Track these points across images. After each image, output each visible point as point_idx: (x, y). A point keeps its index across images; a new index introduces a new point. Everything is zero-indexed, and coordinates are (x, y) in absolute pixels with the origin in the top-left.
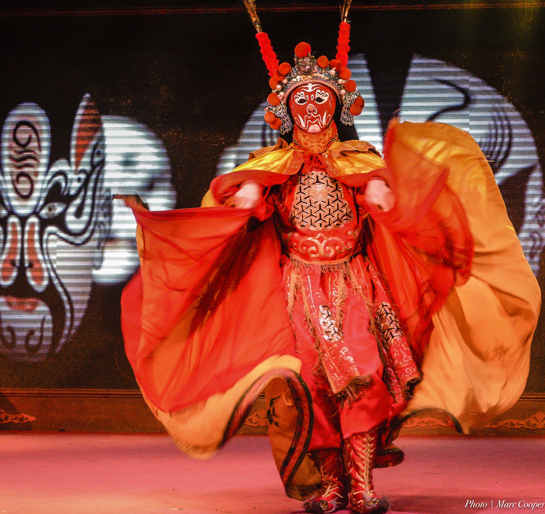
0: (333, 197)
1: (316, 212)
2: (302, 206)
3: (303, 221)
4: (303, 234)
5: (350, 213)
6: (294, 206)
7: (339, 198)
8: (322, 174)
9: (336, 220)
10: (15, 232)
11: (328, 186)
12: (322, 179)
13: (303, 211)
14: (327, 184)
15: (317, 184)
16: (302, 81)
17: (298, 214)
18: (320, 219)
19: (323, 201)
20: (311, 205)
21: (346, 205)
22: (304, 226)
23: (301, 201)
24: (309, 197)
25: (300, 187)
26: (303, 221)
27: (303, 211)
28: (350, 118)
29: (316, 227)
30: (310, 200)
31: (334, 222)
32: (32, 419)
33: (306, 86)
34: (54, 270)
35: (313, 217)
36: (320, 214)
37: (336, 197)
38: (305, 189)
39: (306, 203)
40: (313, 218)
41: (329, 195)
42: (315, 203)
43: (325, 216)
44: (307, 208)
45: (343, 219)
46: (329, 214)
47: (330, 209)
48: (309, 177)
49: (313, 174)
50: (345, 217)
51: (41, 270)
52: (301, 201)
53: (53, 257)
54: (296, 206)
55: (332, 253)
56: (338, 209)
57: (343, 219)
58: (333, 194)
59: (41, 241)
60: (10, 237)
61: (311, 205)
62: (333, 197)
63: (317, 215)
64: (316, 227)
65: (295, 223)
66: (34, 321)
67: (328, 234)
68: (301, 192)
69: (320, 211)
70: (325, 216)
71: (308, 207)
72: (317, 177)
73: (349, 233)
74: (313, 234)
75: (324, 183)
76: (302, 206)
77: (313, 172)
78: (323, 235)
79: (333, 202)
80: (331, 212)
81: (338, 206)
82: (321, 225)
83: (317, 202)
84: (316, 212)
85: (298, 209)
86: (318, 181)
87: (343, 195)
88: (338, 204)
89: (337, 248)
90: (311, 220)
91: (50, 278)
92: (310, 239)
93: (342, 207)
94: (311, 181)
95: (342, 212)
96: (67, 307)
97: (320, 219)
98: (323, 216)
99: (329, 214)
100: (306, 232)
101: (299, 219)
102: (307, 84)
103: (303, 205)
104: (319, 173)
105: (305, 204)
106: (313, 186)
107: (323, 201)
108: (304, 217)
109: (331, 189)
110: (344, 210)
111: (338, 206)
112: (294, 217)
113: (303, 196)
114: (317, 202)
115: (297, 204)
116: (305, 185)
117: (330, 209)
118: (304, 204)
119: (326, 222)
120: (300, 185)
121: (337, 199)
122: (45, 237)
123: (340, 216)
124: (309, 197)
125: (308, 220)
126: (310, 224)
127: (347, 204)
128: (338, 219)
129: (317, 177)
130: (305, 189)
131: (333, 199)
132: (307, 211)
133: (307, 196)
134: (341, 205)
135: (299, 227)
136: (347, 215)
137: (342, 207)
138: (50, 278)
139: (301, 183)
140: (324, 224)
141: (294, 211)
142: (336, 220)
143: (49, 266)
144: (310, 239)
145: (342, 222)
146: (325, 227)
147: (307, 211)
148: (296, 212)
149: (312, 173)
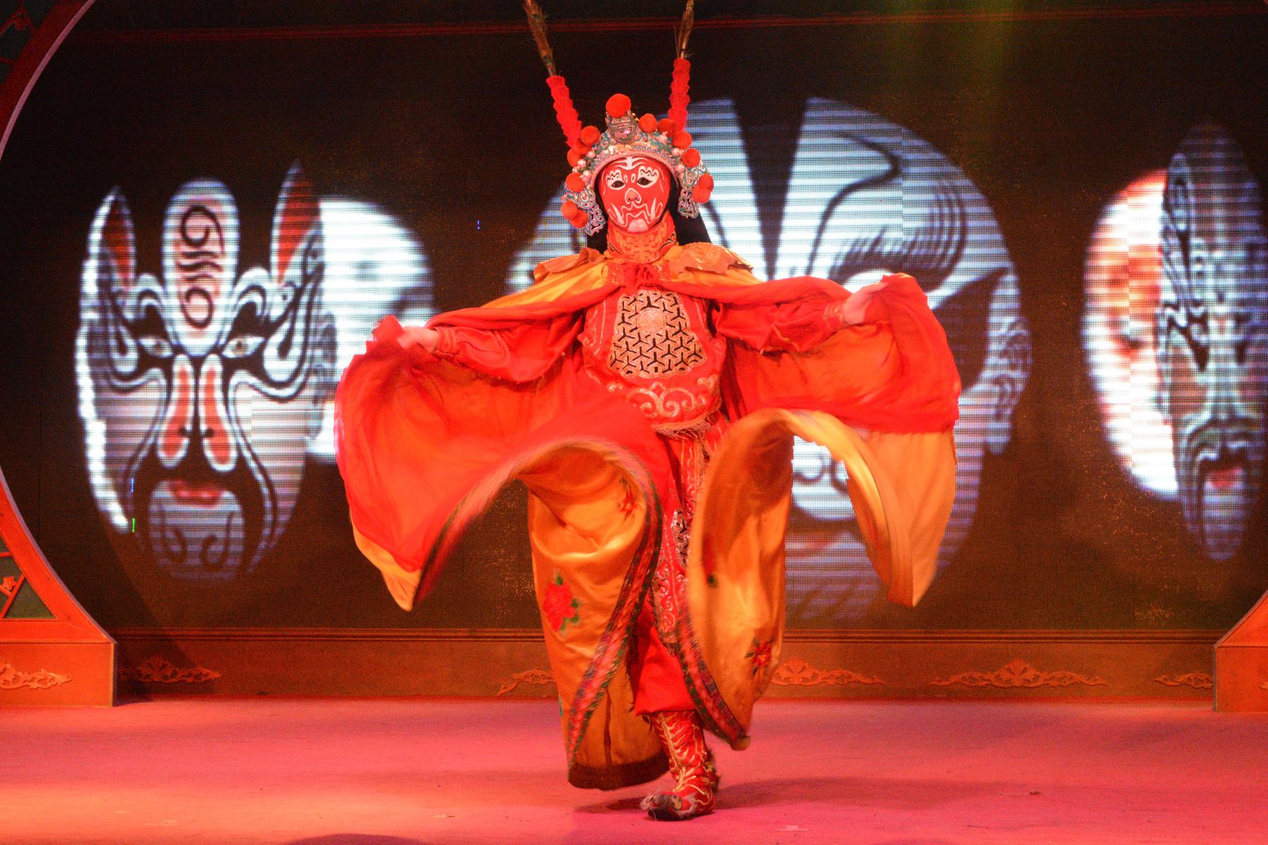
0: (674, 327)
1: (648, 351)
2: (627, 343)
3: (629, 364)
4: (630, 385)
5: (700, 351)
6: (614, 344)
7: (682, 328)
8: (656, 294)
9: (680, 362)
10: (184, 388)
11: (665, 312)
12: (656, 301)
13: (628, 349)
14: (663, 309)
15: (648, 308)
16: (618, 153)
17: (621, 355)
18: (655, 360)
19: (658, 334)
20: (640, 341)
21: (693, 338)
22: (631, 372)
23: (625, 336)
24: (636, 328)
25: (623, 314)
26: (629, 364)
27: (628, 349)
28: (694, 206)
29: (649, 372)
30: (639, 334)
31: (676, 365)
32: (214, 675)
33: (624, 161)
34: (249, 447)
35: (644, 358)
36: (655, 353)
37: (678, 328)
38: (630, 317)
39: (633, 338)
40: (644, 359)
41: (667, 324)
42: (646, 337)
43: (662, 357)
44: (634, 345)
45: (689, 361)
46: (669, 353)
47: (669, 345)
48: (635, 300)
49: (641, 295)
50: (693, 358)
51: (226, 447)
52: (625, 336)
53: (246, 427)
54: (618, 343)
55: (676, 413)
56: (682, 346)
57: (689, 361)
58: (672, 323)
59: (226, 401)
60: (175, 395)
61: (640, 341)
62: (674, 327)
63: (650, 354)
64: (649, 372)
65: (617, 368)
66: (217, 527)
67: (669, 383)
68: (624, 322)
69: (655, 348)
70: (662, 357)
71: (636, 344)
72: (648, 298)
73: (701, 381)
74: (646, 384)
75: (659, 308)
76: (627, 343)
77: (641, 291)
78: (661, 385)
79: (673, 335)
80: (672, 350)
81: (681, 340)
82: (656, 370)
83: (649, 335)
84: (648, 351)
85: (621, 347)
86: (649, 305)
87: (688, 324)
88: (681, 338)
89: (684, 403)
90: (641, 362)
91: (241, 461)
92: (642, 391)
93: (688, 343)
94: (639, 305)
95: (688, 349)
96: (268, 504)
97: (655, 360)
98: (658, 357)
99: (669, 353)
100: (635, 382)
101: (622, 362)
102: (624, 158)
103: (628, 341)
104: (650, 293)
105: (632, 339)
106: (641, 312)
107: (658, 334)
108: (631, 359)
109: (670, 316)
110: (691, 347)
111: (681, 340)
112: (616, 359)
113: (628, 328)
114: (649, 335)
115: (619, 341)
116: (629, 311)
117: (669, 345)
118: (629, 340)
119: (663, 364)
120: (623, 312)
121: (680, 330)
122: (231, 395)
123: (685, 357)
124: (636, 328)
125: (637, 362)
126: (640, 368)
127: (696, 338)
128: (682, 360)
129: (648, 298)
130: (630, 317)
131: (673, 331)
132: (635, 349)
133: (633, 328)
134: (685, 339)
135: (623, 373)
136: (695, 354)
137: (688, 343)
138: (241, 461)
139: (624, 310)
140: (661, 369)
141: (615, 352)
142: (680, 362)
143: (241, 441)
144: (642, 391)
145: (687, 365)
146: (664, 372)
147: (635, 349)
148: (618, 353)
149: (640, 293)
